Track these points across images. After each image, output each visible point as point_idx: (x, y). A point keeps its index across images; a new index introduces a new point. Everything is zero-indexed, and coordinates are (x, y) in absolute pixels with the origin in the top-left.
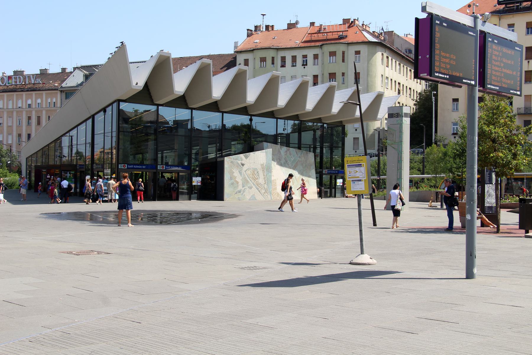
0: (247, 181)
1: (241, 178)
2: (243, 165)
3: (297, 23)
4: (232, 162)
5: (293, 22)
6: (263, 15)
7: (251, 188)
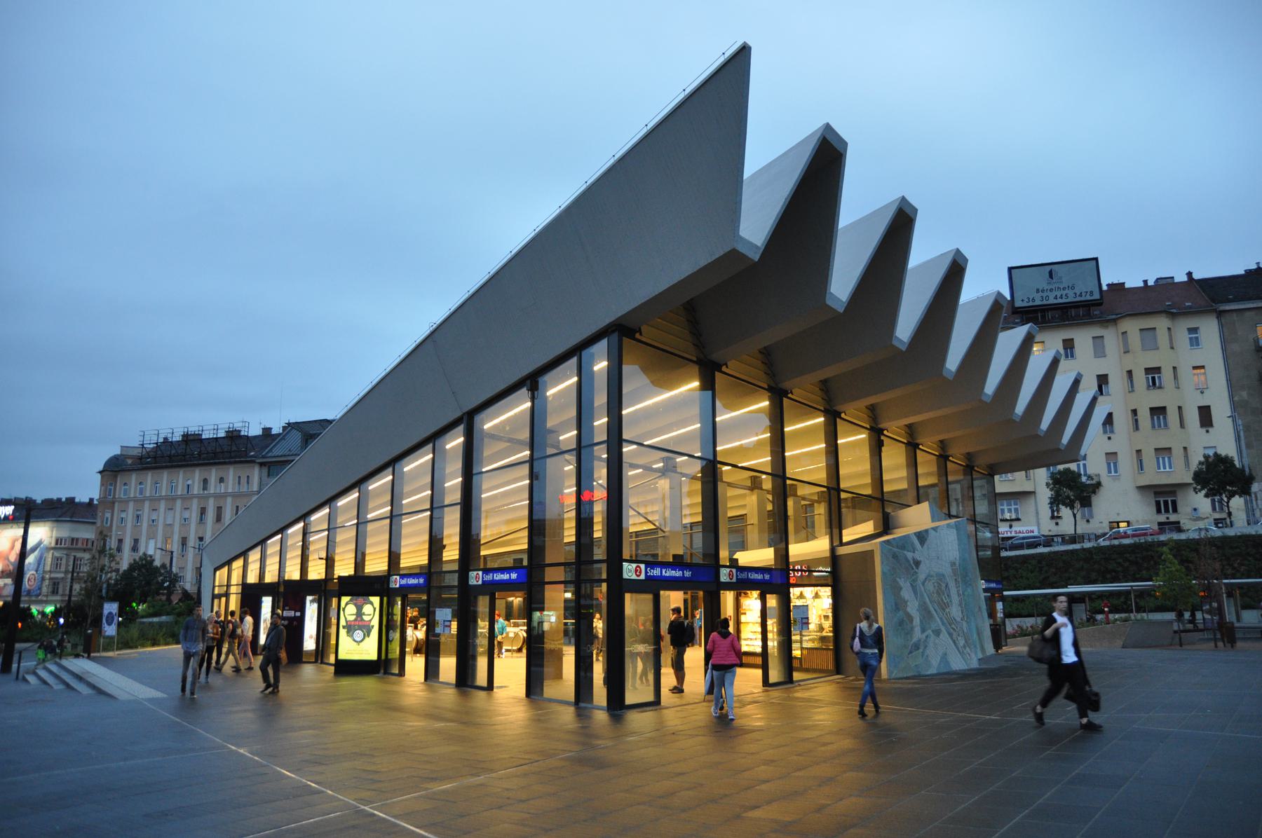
0: (929, 612)
1: (917, 604)
2: (917, 563)
4: (895, 556)
7: (937, 633)
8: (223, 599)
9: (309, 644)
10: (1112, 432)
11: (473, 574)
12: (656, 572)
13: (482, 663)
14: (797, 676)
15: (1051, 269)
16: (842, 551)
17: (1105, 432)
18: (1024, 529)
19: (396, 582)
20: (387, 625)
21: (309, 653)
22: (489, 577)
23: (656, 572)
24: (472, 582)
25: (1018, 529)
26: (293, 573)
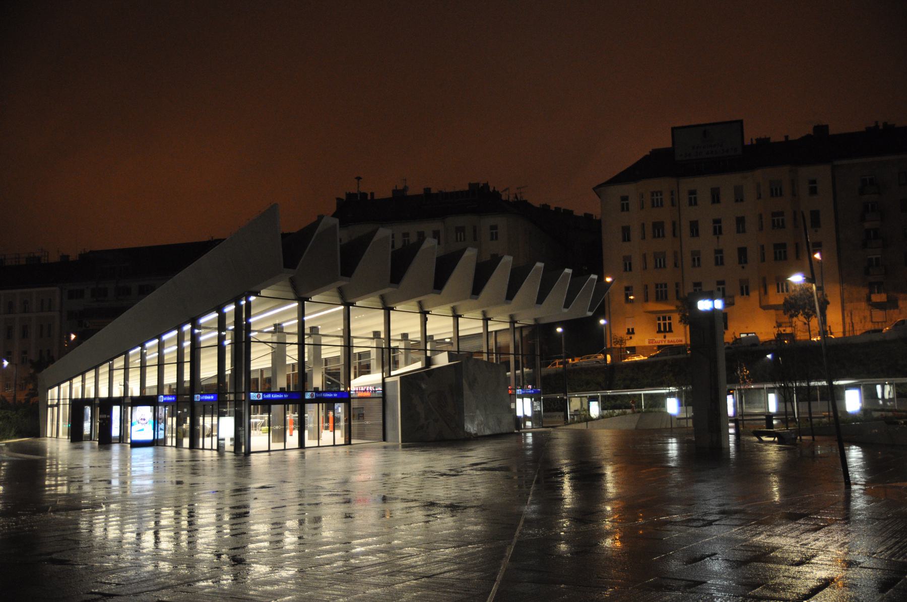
3: (405, 189)
5: (400, 187)
6: (359, 178)
8: (56, 409)
9: (115, 432)
10: (746, 262)
11: (196, 396)
12: (269, 396)
13: (201, 440)
14: (353, 442)
15: (705, 130)
16: (388, 380)
17: (740, 262)
18: (675, 339)
19: (162, 399)
20: (156, 420)
21: (115, 438)
22: (203, 398)
23: (269, 396)
24: (196, 400)
25: (670, 339)
26: (104, 393)
